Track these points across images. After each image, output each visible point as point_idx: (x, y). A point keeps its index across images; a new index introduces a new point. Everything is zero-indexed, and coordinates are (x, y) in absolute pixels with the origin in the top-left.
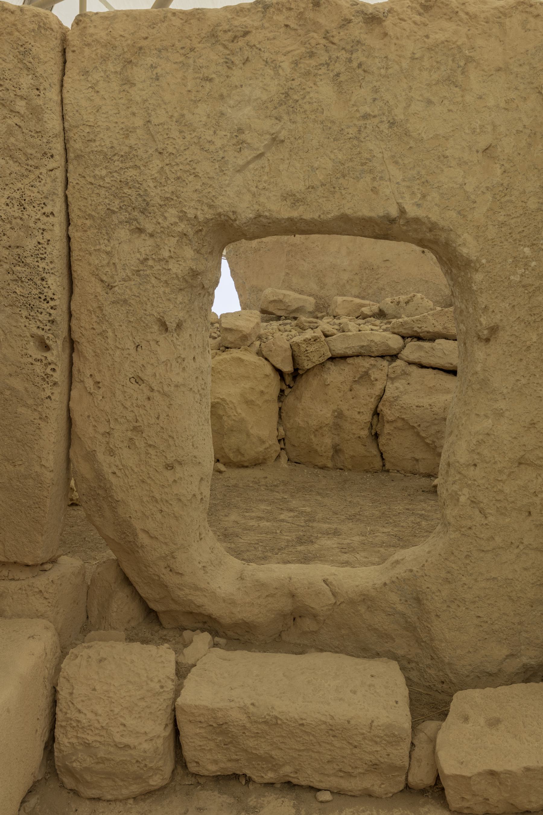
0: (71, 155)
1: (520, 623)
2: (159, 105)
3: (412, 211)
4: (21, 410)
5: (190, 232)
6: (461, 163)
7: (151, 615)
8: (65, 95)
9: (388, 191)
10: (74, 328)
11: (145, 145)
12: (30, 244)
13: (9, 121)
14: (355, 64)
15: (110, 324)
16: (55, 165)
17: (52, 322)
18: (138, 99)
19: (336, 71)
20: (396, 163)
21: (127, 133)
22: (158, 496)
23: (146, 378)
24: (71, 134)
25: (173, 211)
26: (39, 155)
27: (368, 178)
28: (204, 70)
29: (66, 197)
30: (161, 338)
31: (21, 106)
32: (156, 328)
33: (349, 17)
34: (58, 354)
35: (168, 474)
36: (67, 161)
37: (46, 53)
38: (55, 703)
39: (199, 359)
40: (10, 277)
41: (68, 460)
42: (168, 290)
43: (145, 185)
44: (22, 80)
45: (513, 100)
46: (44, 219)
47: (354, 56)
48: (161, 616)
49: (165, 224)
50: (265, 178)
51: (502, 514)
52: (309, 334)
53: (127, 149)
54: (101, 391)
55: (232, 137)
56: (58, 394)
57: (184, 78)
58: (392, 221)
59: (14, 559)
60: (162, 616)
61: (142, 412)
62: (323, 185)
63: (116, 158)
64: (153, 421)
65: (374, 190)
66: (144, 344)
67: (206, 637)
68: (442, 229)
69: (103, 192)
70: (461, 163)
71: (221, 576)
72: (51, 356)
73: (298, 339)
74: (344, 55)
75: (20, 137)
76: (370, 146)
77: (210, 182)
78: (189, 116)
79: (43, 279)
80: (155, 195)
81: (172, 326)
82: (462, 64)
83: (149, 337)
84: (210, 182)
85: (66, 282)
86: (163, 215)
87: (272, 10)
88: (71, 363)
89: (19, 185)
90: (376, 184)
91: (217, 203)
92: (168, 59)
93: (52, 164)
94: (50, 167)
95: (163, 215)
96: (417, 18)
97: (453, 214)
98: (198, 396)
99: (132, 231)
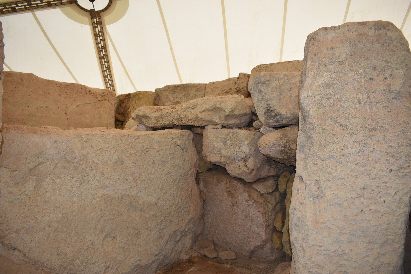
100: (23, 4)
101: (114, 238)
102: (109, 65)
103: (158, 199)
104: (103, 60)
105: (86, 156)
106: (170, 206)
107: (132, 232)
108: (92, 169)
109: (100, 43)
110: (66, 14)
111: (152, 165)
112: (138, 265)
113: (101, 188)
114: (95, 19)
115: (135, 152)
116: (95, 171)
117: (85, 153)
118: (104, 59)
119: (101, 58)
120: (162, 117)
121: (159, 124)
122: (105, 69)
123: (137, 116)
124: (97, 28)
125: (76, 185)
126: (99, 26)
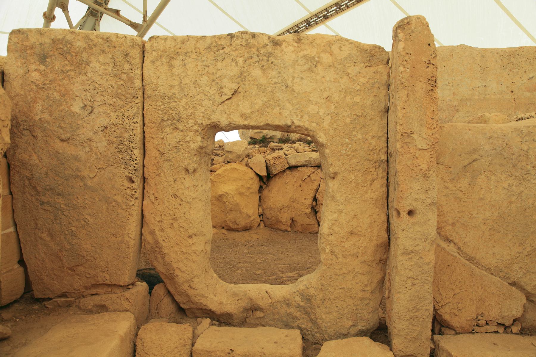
0: (146, 96)
1: (356, 309)
2: (186, 76)
3: (297, 123)
5: (200, 130)
6: (317, 103)
10: (145, 172)
12: (126, 136)
13: (119, 83)
14: (270, 62)
15: (163, 170)
16: (138, 101)
17: (136, 170)
18: (176, 73)
19: (262, 64)
20: (289, 102)
21: (172, 87)
22: (185, 251)
23: (179, 195)
24: (146, 87)
25: (192, 121)
26: (132, 97)
27: (278, 108)
28: (205, 62)
29: (143, 114)
30: (186, 177)
31: (124, 76)
32: (184, 172)
34: (138, 184)
35: (190, 241)
36: (144, 98)
37: (136, 53)
38: (135, 351)
39: (204, 186)
40: (116, 150)
41: (141, 234)
42: (189, 155)
43: (179, 109)
44: (125, 66)
45: (336, 78)
46: (133, 125)
47: (270, 59)
49: (188, 126)
50: (233, 107)
53: (171, 94)
54: (158, 201)
55: (217, 91)
56: (138, 203)
57: (197, 65)
58: (290, 126)
60: (187, 311)
61: (177, 211)
62: (258, 111)
63: (166, 98)
64: (182, 215)
66: (178, 180)
67: (208, 320)
68: (311, 130)
69: (160, 112)
70: (317, 103)
72: (134, 186)
73: (270, 156)
74: (265, 58)
75: (123, 90)
76: (278, 95)
77: (208, 109)
78: (199, 81)
79: (132, 151)
80: (184, 114)
81: (191, 171)
82: (315, 63)
83: (181, 176)
84: (208, 109)
85: (142, 151)
86: (187, 122)
87: (235, 38)
88: (144, 188)
89: (122, 110)
90: (281, 111)
91: (212, 117)
92: (189, 57)
93: (137, 101)
95: (187, 122)
96: (296, 44)
97: (314, 124)
99: (173, 129)
105: (526, 151)
117: (525, 148)
125: (515, 184)
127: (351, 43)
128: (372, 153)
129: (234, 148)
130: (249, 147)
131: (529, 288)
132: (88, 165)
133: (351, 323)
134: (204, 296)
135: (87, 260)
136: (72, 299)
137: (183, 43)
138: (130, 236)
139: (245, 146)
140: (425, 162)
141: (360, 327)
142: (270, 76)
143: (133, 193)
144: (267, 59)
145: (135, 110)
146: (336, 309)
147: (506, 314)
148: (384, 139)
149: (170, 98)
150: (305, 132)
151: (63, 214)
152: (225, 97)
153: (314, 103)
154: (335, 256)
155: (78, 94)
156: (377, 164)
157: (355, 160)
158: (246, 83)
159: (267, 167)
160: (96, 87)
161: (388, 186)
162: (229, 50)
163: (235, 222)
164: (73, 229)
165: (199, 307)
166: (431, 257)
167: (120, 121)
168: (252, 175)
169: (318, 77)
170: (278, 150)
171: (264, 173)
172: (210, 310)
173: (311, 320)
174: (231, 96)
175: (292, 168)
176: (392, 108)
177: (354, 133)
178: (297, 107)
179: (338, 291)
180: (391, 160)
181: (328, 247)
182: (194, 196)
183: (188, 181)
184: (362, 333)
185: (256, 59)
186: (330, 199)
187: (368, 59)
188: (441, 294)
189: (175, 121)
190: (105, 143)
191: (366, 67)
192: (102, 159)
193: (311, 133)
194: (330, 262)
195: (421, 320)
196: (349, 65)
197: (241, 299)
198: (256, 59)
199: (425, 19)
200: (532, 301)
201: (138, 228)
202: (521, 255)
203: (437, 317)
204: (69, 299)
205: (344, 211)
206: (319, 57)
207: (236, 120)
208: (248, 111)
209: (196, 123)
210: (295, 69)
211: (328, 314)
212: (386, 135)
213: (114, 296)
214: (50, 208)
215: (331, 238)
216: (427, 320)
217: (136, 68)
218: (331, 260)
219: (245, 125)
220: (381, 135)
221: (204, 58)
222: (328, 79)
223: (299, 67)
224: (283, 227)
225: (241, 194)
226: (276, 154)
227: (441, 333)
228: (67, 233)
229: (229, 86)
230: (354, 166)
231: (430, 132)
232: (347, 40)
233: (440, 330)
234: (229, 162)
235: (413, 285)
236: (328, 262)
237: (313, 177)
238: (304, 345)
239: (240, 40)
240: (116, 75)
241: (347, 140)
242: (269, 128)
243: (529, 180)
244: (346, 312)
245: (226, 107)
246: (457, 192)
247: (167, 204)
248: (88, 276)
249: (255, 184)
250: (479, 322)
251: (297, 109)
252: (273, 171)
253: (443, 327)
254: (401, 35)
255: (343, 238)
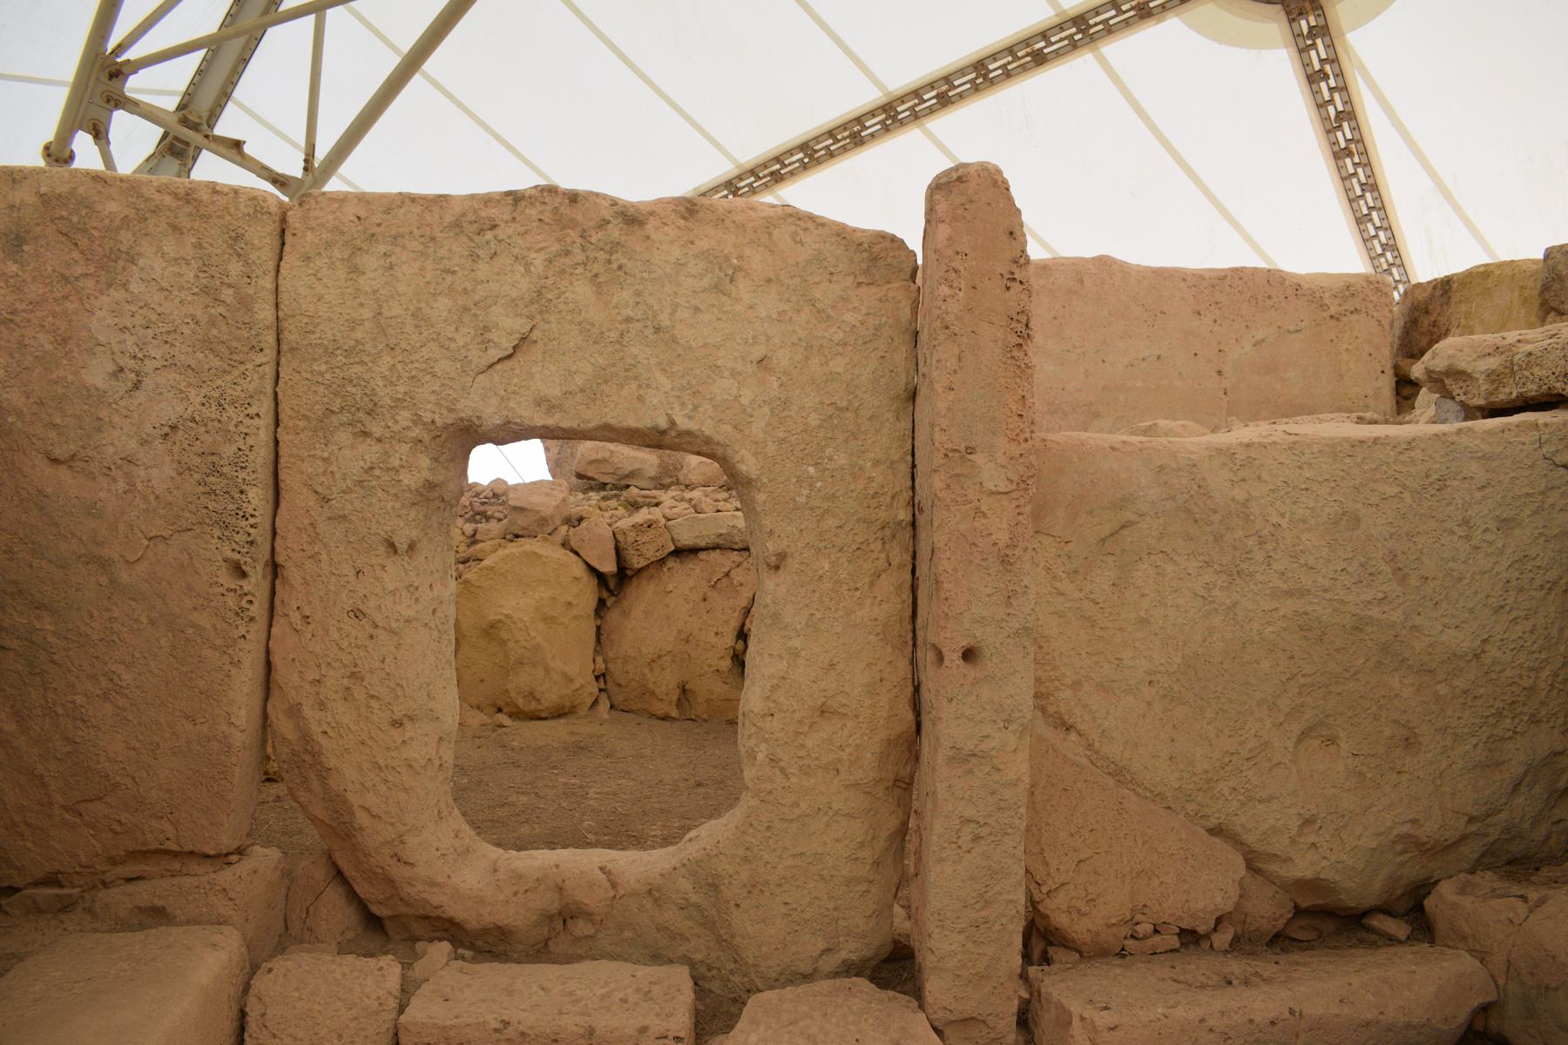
0: (284, 347)
1: (836, 909)
2: (392, 297)
3: (683, 423)
4: (207, 652)
5: (426, 437)
6: (734, 374)
7: (373, 923)
8: (281, 281)
9: (655, 401)
10: (278, 549)
11: (374, 340)
12: (229, 450)
13: (213, 311)
14: (615, 266)
15: (325, 545)
16: (264, 360)
17: (252, 543)
18: (369, 289)
20: (664, 370)
21: (354, 324)
24: (285, 324)
25: (406, 414)
27: (634, 387)
29: (276, 394)
31: (228, 294)
32: (382, 549)
33: (608, 217)
34: (257, 581)
35: (396, 734)
40: (201, 489)
41: (265, 716)
42: (398, 505)
43: (372, 384)
44: (231, 267)
46: (247, 421)
48: (388, 924)
49: (396, 428)
51: (806, 774)
52: (643, 515)
53: (352, 343)
54: (310, 628)
56: (256, 633)
57: (422, 269)
58: (663, 433)
59: (189, 847)
60: (388, 921)
61: (362, 654)
62: (582, 391)
64: (377, 665)
65: (640, 399)
67: (446, 946)
69: (322, 389)
70: (734, 374)
71: (466, 869)
72: (247, 585)
73: (625, 523)
74: (602, 256)
75: (224, 328)
76: (635, 350)
80: (385, 396)
82: (730, 272)
83: (374, 561)
85: (270, 493)
87: (524, 203)
88: (273, 593)
89: (219, 382)
91: (459, 406)
92: (404, 247)
93: (260, 359)
94: (258, 362)
97: (728, 428)
98: (435, 633)
99: (355, 435)
100: (1063, 35)
101: (1332, 740)
102: (1371, 175)
103: (1484, 641)
104: (1348, 161)
105: (1244, 505)
106: (1531, 669)
107: (1388, 731)
108: (1262, 542)
109: (1331, 101)
110: (1201, 29)
111: (1460, 532)
112: (1408, 836)
113: (1289, 594)
114: (1303, 23)
115: (1396, 490)
116: (1269, 546)
117: (1241, 495)
118: (1350, 154)
119: (1339, 154)
120: (1512, 372)
121: (1502, 397)
122: (1359, 192)
123: (1429, 372)
124: (1313, 53)
125: (1219, 583)
126: (1319, 41)
127: (823, 225)
128: (874, 503)
129: (532, 500)
130: (571, 499)
131: (1251, 839)
132: (122, 527)
133: (821, 946)
134: (433, 883)
135: (117, 786)
136: (75, 891)
137: (388, 211)
138: (233, 720)
139: (561, 495)
140: (1004, 525)
141: (844, 955)
142: (615, 300)
143: (244, 603)
144: (606, 256)
145: (254, 384)
146: (784, 909)
147: (1201, 905)
148: (904, 468)
149: (348, 353)
150: (704, 449)
151: (53, 661)
152: (494, 354)
153: (726, 373)
154: (782, 770)
155: (102, 339)
156: (888, 532)
157: (831, 522)
158: (552, 318)
159: (618, 552)
160: (150, 321)
161: (914, 589)
162: (510, 231)
163: (531, 695)
164: (79, 700)
165: (421, 911)
166: (1019, 767)
167: (212, 413)
168: (579, 570)
169: (738, 308)
170: (649, 505)
171: (608, 566)
172: (451, 921)
173: (719, 940)
174: (511, 351)
175: (681, 553)
176: (923, 391)
177: (829, 451)
178: (684, 381)
179: (790, 862)
180: (921, 520)
181: (763, 746)
182: (411, 613)
183: (393, 574)
184: (850, 969)
185: (579, 256)
186: (769, 621)
187: (864, 266)
188: (1046, 863)
189: (361, 414)
190: (169, 470)
191: (859, 284)
192: (162, 512)
193: (720, 451)
194: (768, 786)
195: (997, 927)
196: (817, 279)
197: (534, 890)
198: (579, 256)
199: (999, 172)
200: (1258, 871)
201: (256, 702)
202: (1234, 758)
203: (1038, 920)
204: (66, 891)
205: (803, 653)
206: (740, 257)
207: (524, 413)
208: (554, 391)
209: (417, 420)
210: (679, 284)
211: (763, 921)
212: (909, 458)
213: (187, 882)
214: (15, 644)
215: (774, 724)
216: (1011, 927)
217: (259, 272)
218: (771, 780)
219: (545, 427)
220: (896, 458)
221: (443, 252)
222: (763, 314)
223: (690, 280)
224: (660, 708)
225: (548, 620)
226: (643, 515)
227: (1046, 960)
228: (60, 710)
229: (507, 325)
230: (827, 536)
231: (1014, 450)
232: (812, 218)
233: (1045, 952)
234: (517, 536)
235: (977, 838)
236: (763, 786)
237: (738, 575)
238: (701, 1007)
239: (539, 207)
240: (205, 290)
241: (811, 470)
242: (613, 436)
243: (1251, 574)
244: (807, 915)
245: (496, 378)
246: (1086, 604)
247: (336, 636)
248: (118, 828)
249: (588, 593)
250: (1138, 928)
251: (682, 389)
252: (635, 561)
253: (1051, 944)
254: (942, 208)
255: (800, 722)
